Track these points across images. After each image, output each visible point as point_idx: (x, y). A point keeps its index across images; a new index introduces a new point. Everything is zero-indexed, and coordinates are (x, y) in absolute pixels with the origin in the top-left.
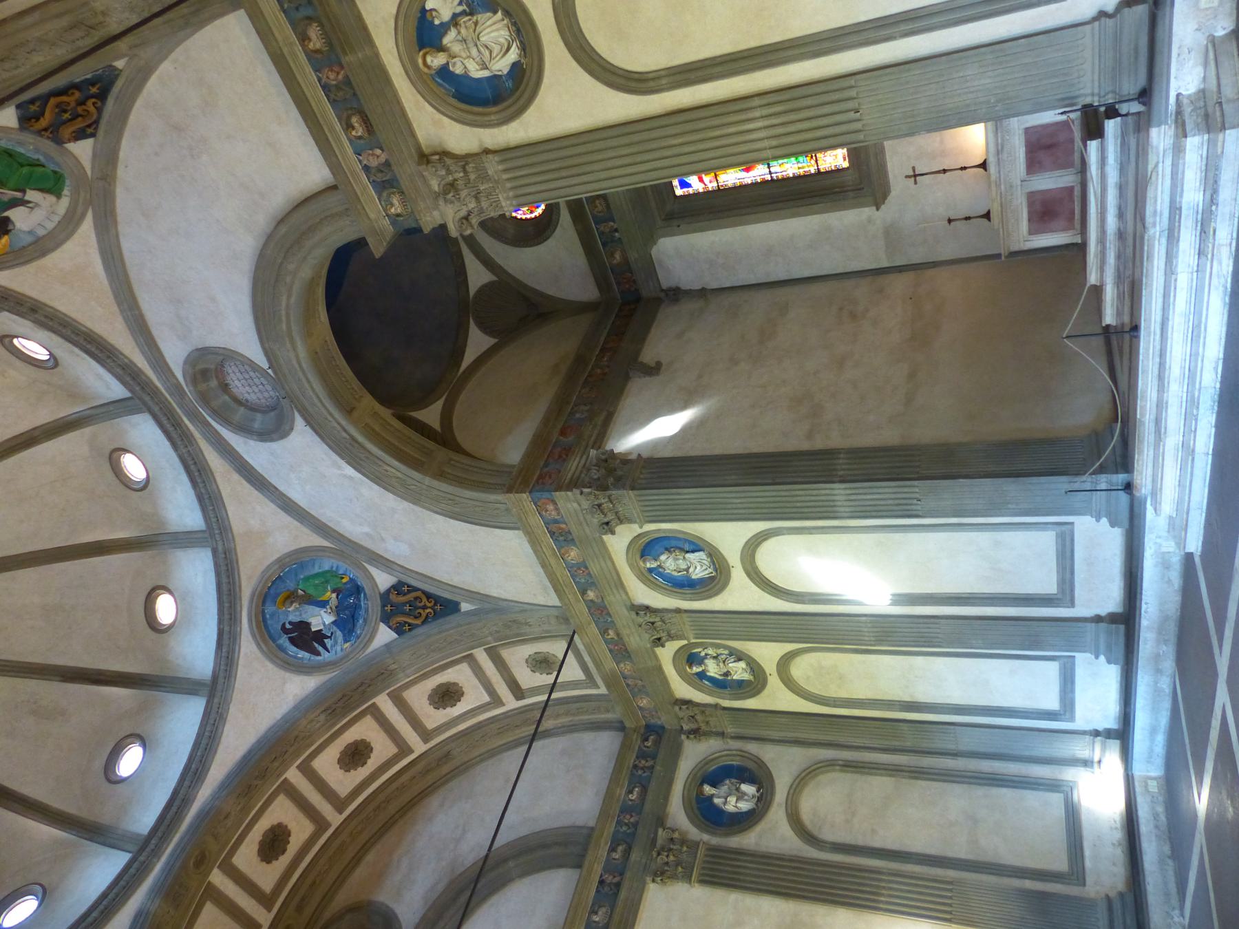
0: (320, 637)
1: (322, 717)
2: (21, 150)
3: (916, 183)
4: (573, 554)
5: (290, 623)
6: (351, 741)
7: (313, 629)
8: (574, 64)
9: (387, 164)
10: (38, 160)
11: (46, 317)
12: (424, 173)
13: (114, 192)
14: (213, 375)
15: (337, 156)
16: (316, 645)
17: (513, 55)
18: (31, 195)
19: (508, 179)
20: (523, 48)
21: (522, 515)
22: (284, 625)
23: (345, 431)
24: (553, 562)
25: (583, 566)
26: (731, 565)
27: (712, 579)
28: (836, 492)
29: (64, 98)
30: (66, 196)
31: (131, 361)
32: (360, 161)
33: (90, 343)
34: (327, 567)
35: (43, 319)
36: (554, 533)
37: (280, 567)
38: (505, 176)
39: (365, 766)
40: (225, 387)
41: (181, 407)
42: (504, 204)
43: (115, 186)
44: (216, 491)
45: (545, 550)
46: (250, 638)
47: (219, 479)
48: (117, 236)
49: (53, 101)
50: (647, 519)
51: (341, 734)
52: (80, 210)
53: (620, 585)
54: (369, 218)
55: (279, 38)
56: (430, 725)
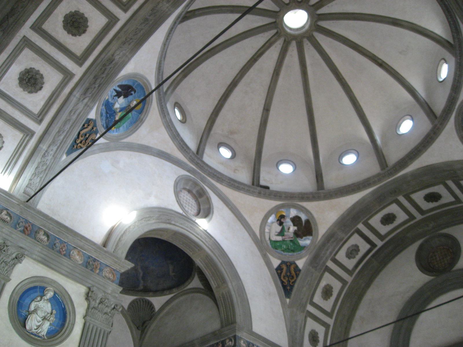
0: (119, 95)
1: (117, 58)
2: (290, 254)
4: (78, 258)
5: (132, 94)
6: (83, 36)
7: (122, 97)
10: (284, 252)
11: (255, 192)
16: (120, 90)
18: (279, 238)
21: (116, 260)
22: (135, 92)
23: (174, 225)
24: (82, 244)
25: (68, 255)
27: (24, 326)
29: (293, 280)
30: (268, 241)
31: (222, 184)
32: (255, 345)
33: (237, 186)
34: (121, 128)
35: (255, 191)
36: (94, 262)
37: (142, 119)
39: (64, 15)
40: (189, 191)
41: (199, 173)
43: (261, 255)
44: (175, 142)
45: (90, 247)
46: (151, 82)
47: (175, 148)
48: (250, 235)
50: (88, 324)
51: (93, 40)
53: (45, 262)
54: (245, 332)
56: (27, 52)
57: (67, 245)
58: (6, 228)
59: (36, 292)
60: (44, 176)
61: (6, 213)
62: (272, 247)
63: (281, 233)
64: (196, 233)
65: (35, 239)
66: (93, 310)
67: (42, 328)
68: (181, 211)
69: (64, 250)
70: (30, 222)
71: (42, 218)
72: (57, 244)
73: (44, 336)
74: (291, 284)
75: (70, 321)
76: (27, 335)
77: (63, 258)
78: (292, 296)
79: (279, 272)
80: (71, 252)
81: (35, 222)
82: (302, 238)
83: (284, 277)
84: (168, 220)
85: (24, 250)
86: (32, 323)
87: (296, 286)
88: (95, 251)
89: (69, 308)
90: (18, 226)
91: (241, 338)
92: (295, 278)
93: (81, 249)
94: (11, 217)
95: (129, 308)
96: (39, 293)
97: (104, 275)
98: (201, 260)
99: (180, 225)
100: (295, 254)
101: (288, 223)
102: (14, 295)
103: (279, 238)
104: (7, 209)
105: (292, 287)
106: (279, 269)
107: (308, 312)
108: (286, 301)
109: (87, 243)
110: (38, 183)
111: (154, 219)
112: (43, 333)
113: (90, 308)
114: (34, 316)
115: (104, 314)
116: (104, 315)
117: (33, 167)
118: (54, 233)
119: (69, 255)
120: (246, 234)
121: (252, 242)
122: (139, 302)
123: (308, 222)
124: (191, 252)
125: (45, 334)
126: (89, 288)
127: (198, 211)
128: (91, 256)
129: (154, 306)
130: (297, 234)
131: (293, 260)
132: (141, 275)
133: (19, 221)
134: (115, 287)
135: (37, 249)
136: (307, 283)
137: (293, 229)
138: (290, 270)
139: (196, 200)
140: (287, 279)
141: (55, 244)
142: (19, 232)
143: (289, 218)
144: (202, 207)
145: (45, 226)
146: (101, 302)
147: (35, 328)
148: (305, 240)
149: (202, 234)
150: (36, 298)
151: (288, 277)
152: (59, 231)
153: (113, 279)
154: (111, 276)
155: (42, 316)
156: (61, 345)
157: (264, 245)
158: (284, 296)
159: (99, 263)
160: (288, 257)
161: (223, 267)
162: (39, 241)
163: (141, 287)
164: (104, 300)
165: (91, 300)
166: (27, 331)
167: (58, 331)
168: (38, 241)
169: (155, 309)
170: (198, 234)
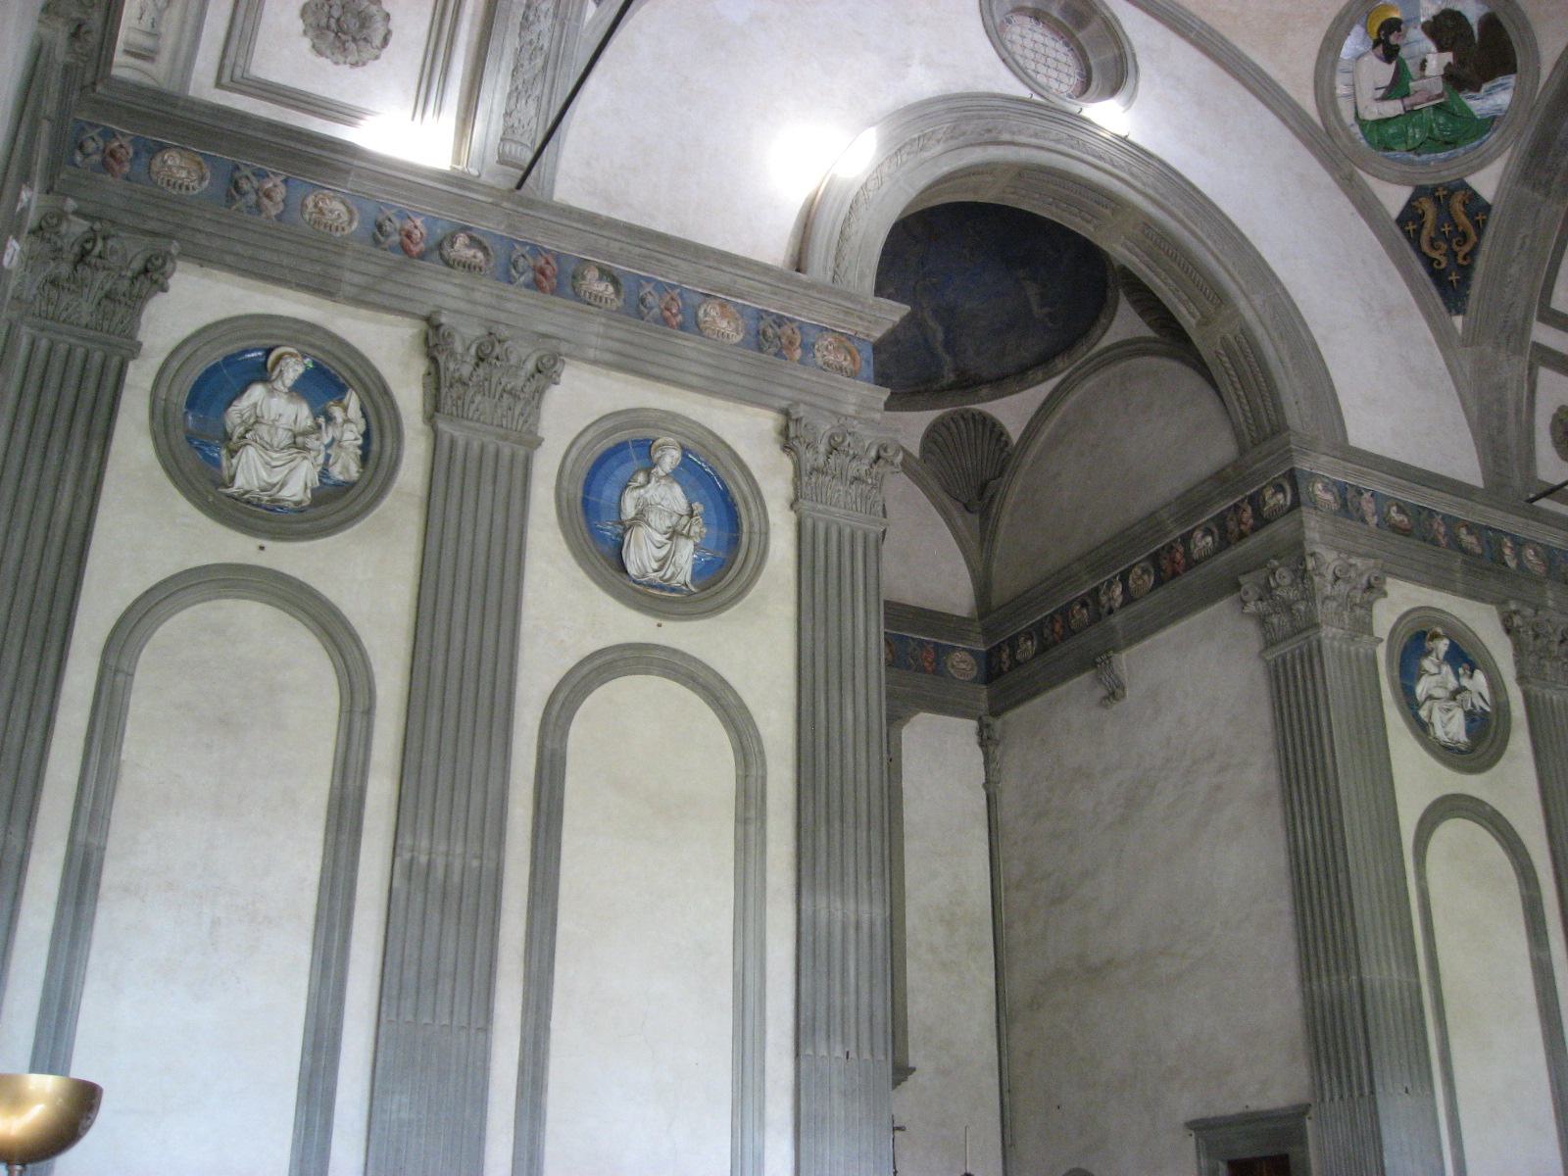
2: (1441, 155)
3: (899, 1129)
4: (726, 327)
8: (1438, 794)
9: (1363, 520)
10: (1419, 155)
12: (1373, 561)
13: (1332, 174)
14: (1061, 19)
15: (1383, 472)
17: (1439, 732)
18: (1393, 108)
19: (1349, 652)
20: (1447, 748)
21: (850, 306)
24: (724, 279)
25: (692, 325)
26: (665, 623)
27: (623, 569)
28: (865, 907)
29: (1467, 248)
36: (779, 326)
38: (1352, 648)
40: (1038, 15)
42: (1334, 630)
43: (1336, 180)
48: (1284, 120)
49: (1473, 238)
50: (809, 523)
52: (1332, 118)
54: (1328, 455)
55: (1480, 507)
57: (680, 295)
58: (483, 289)
59: (628, 459)
60: (546, 91)
61: (467, 242)
62: (1369, 142)
63: (1397, 88)
64: (1094, 156)
65: (577, 296)
66: (813, 480)
67: (674, 565)
68: (1024, 92)
69: (674, 311)
70: (548, 251)
71: (580, 226)
72: (650, 299)
73: (686, 585)
74: (1460, 261)
75: (751, 525)
76: (637, 591)
77: (676, 337)
78: (1472, 303)
79: (1411, 227)
80: (701, 313)
81: (563, 245)
82: (1478, 90)
83: (1432, 242)
84: (989, 131)
85: (554, 341)
86: (643, 554)
87: (1480, 264)
88: (776, 294)
89: (738, 490)
90: (513, 271)
91: (1312, 475)
92: (1473, 238)
93: (727, 294)
94: (484, 249)
95: (924, 449)
96: (636, 464)
97: (820, 362)
98: (1128, 243)
99: (1034, 141)
100: (1461, 150)
101: (1417, 44)
102: (565, 484)
103: (1393, 108)
104: (465, 229)
105: (1466, 272)
106: (1410, 217)
107: (1537, 346)
108: (1453, 325)
109: (739, 272)
110: (535, 120)
111: (938, 141)
112: (680, 578)
113: (803, 473)
114: (641, 532)
115: (852, 483)
116: (853, 487)
117: (503, 70)
118: (628, 266)
119: (697, 325)
120: (1271, 121)
121: (1298, 143)
122: (952, 425)
123: (1490, 23)
124: (1088, 222)
125: (688, 580)
126: (786, 413)
127: (1080, 75)
128: (762, 310)
129: (1001, 426)
130: (1455, 79)
131: (1458, 177)
132: (940, 336)
133: (514, 257)
134: (865, 392)
135: (593, 329)
136: (1522, 247)
137: (1437, 61)
138: (1450, 215)
139: (1066, 39)
140: (1444, 246)
141: (642, 301)
142: (524, 289)
143: (1419, 27)
144: (1092, 62)
145: (594, 252)
146: (833, 449)
147: (655, 566)
148: (1489, 93)
149: (1112, 150)
150: (631, 479)
151: (1449, 241)
152: (645, 257)
153: (851, 366)
154: (845, 359)
155: (665, 529)
156: (744, 601)
157: (1337, 142)
158: (1443, 308)
159: (797, 324)
160: (1437, 168)
161: (1209, 249)
162: (592, 301)
163: (950, 377)
164: (840, 440)
165: (802, 449)
166: (634, 581)
167: (724, 561)
168: (589, 304)
169: (1008, 437)
170: (1100, 158)
